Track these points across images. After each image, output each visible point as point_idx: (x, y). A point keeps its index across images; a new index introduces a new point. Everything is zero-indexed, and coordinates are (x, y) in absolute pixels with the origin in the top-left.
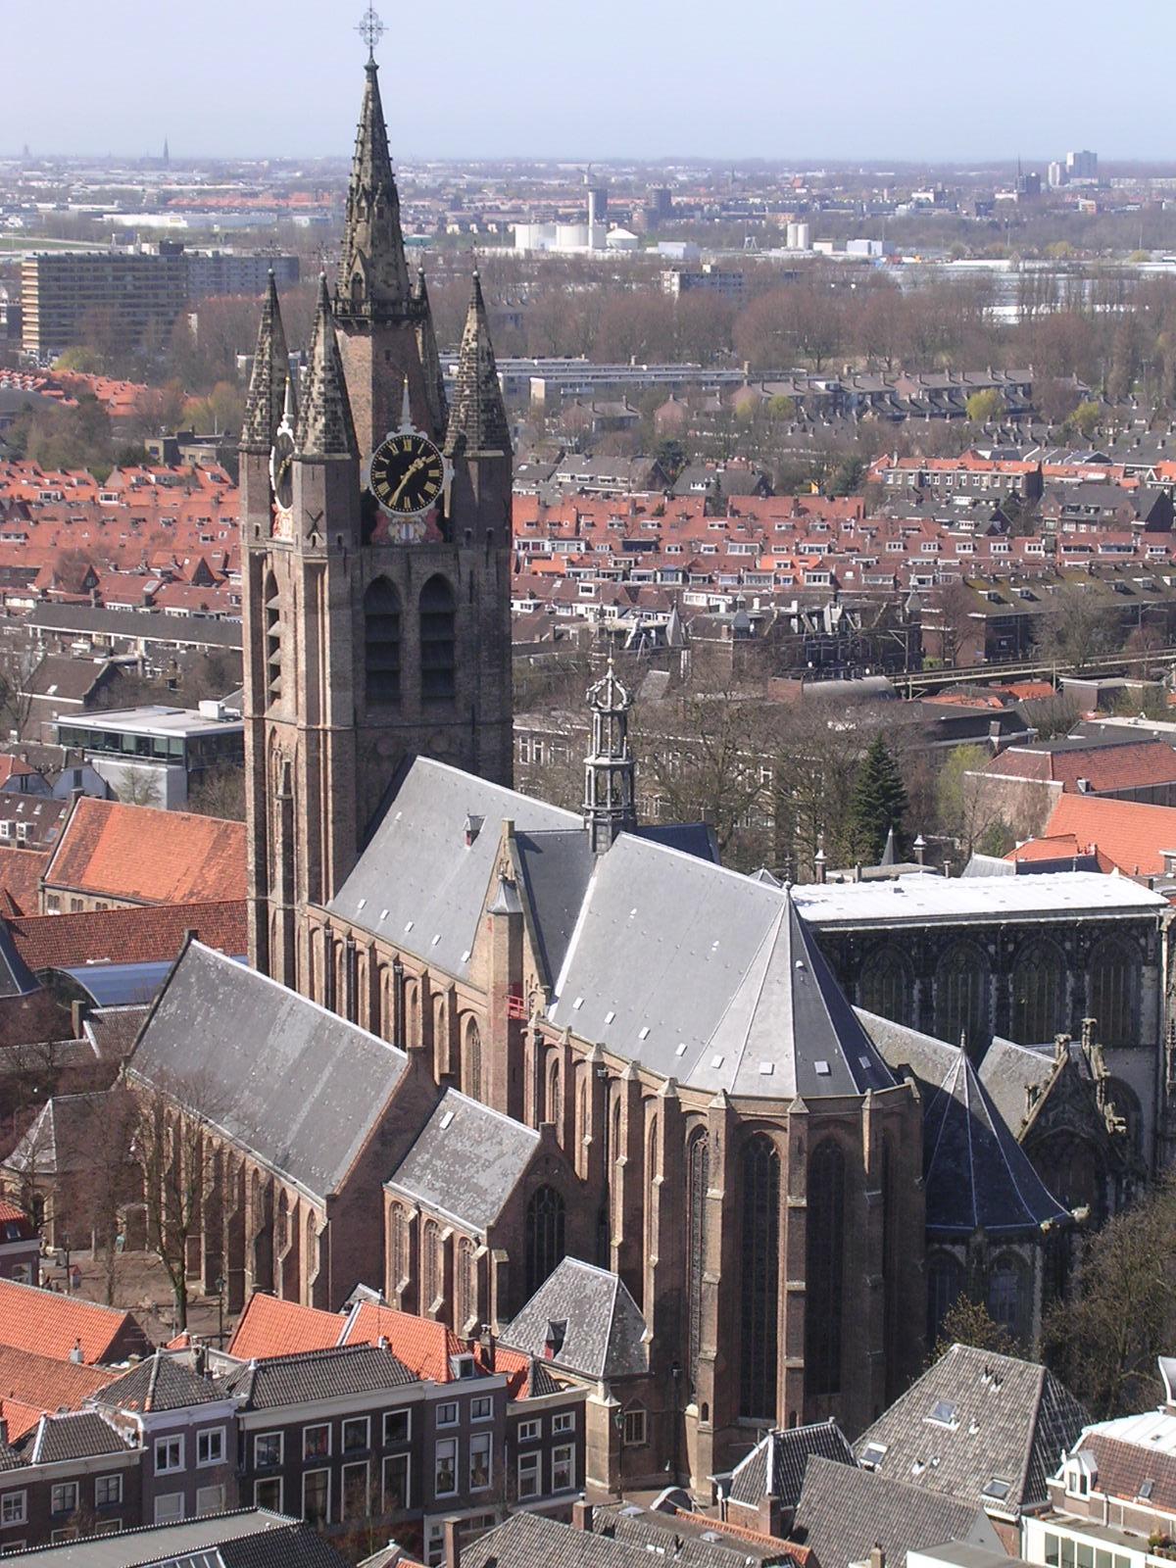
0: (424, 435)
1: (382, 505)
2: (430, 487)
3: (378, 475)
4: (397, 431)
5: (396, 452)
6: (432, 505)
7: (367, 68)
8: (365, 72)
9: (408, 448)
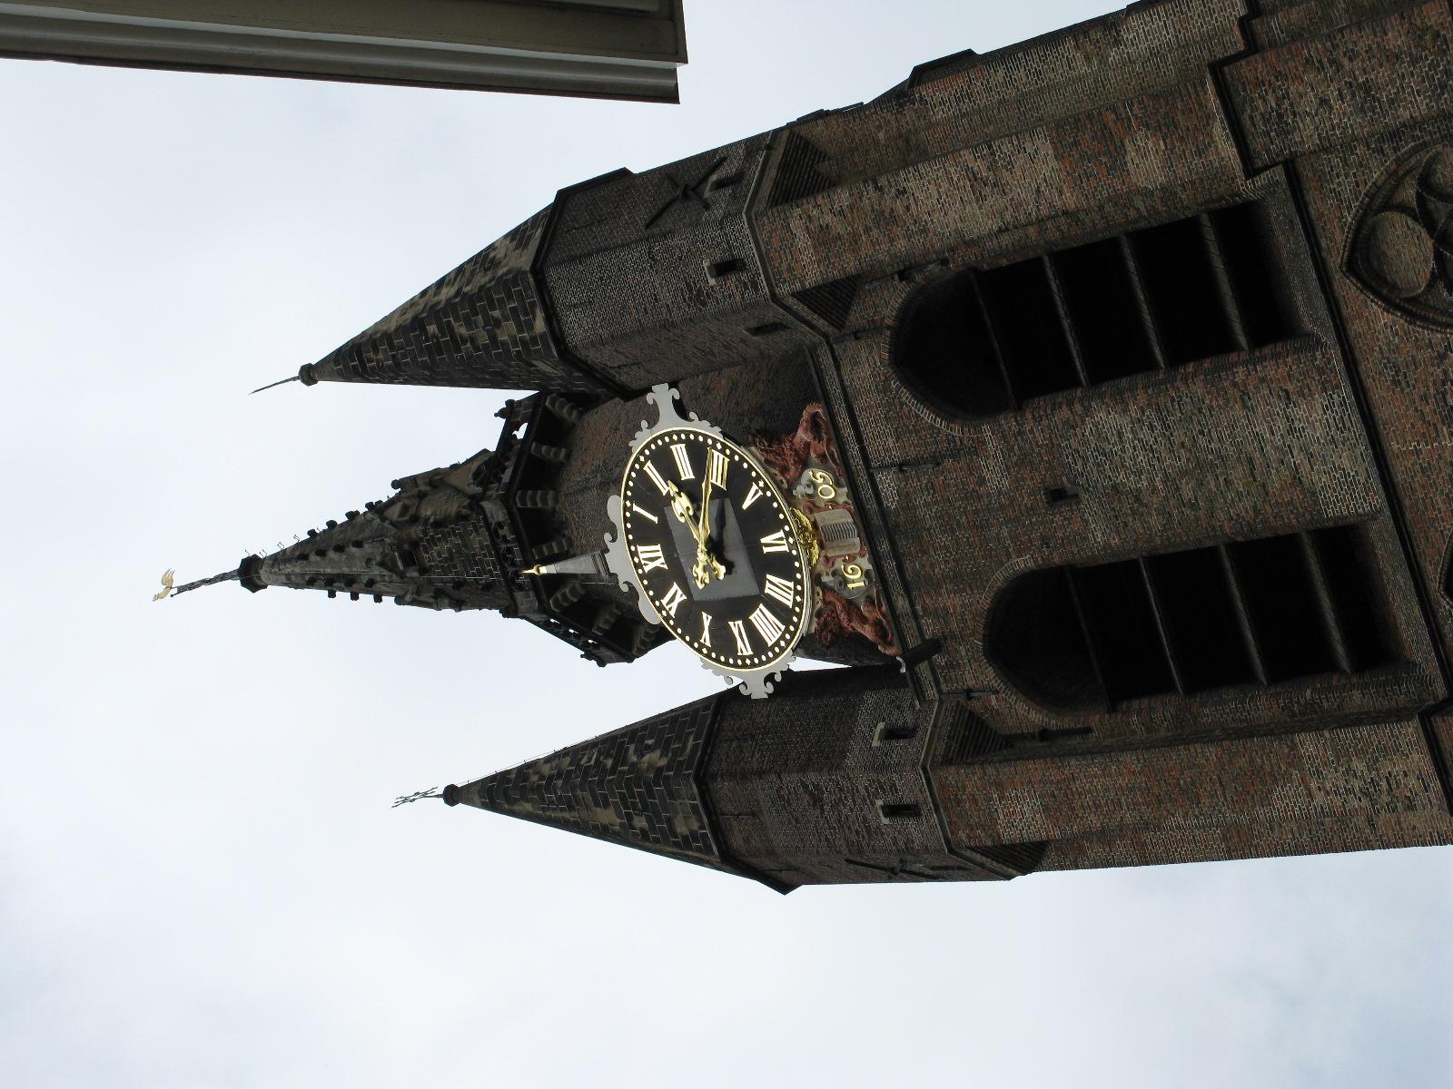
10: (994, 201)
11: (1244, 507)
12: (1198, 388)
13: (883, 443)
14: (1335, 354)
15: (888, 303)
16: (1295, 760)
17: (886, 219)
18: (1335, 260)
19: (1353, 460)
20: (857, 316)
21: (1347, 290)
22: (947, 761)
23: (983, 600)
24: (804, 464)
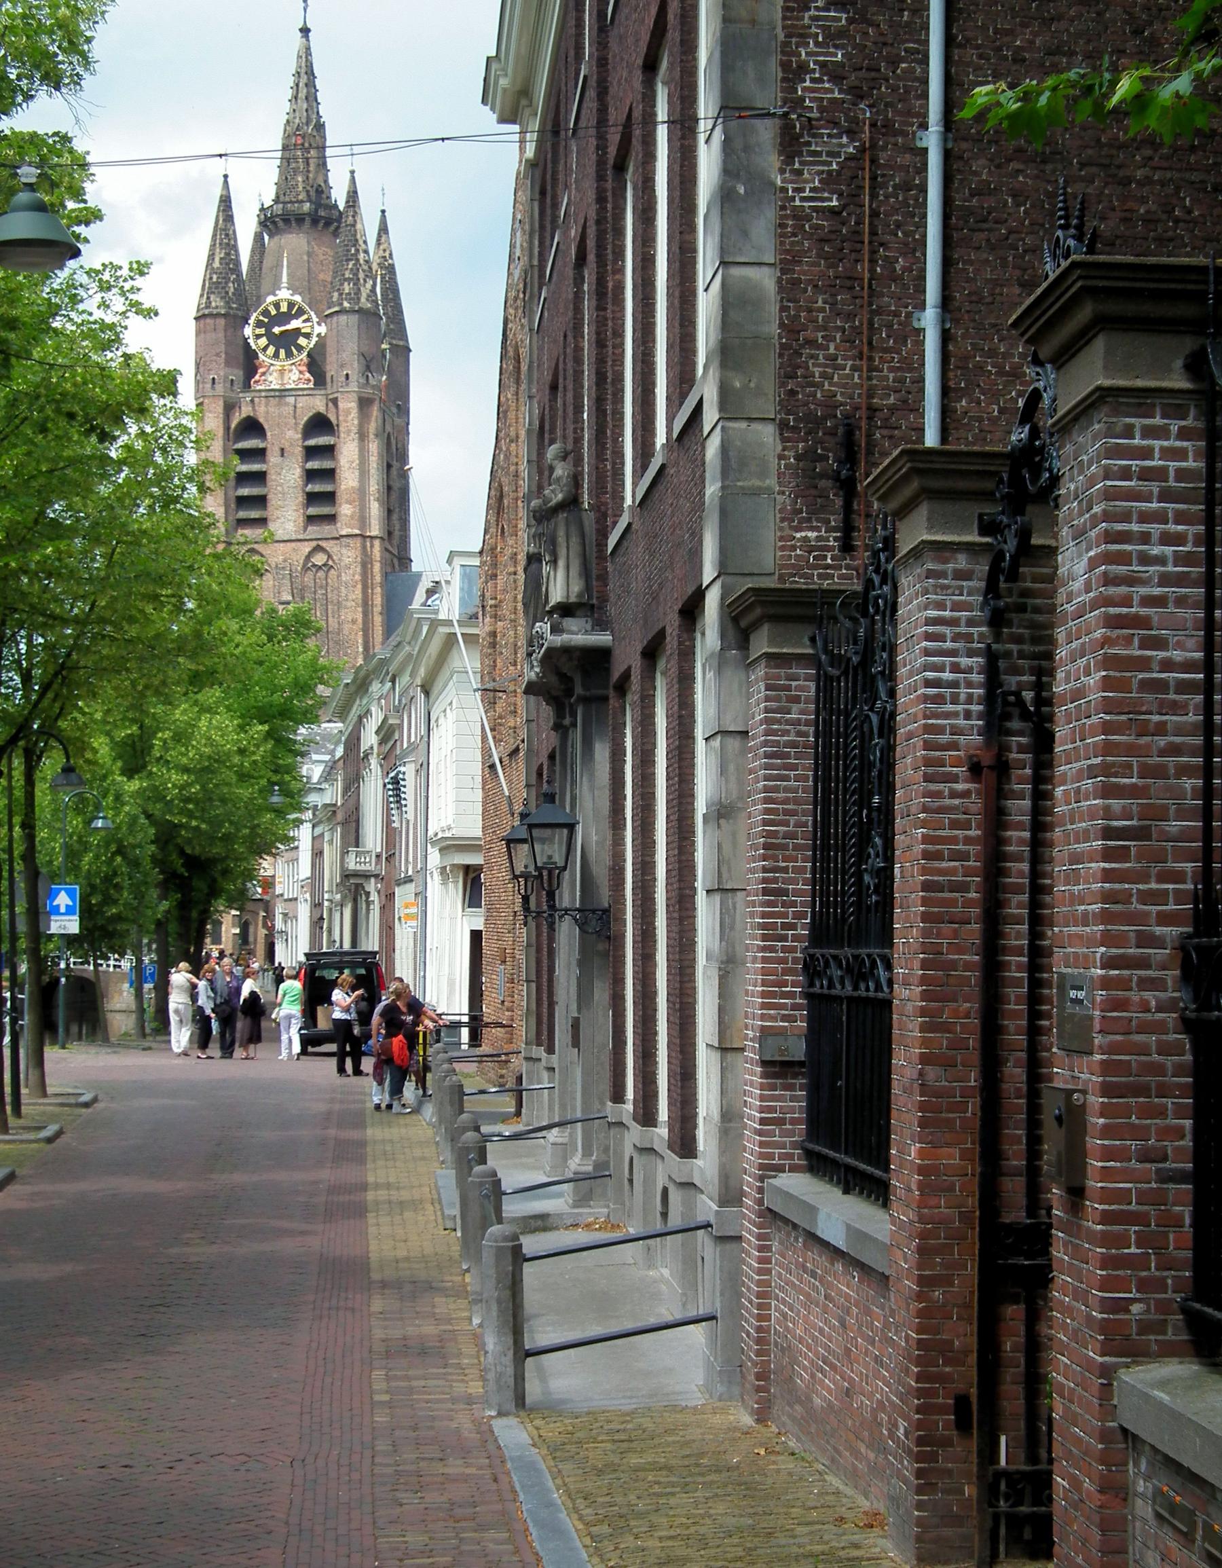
0: (298, 298)
1: (260, 355)
2: (302, 341)
3: (258, 331)
4: (275, 295)
5: (274, 312)
6: (304, 355)
7: (301, 30)
8: (300, 34)
9: (284, 308)
10: (347, 466)
11: (273, 502)
12: (301, 499)
13: (302, 402)
14: (301, 537)
15: (333, 419)
16: (219, 505)
17: (349, 432)
18: (320, 543)
19: (280, 535)
20: (330, 404)
21: (314, 544)
22: (225, 402)
23: (261, 420)
24: (301, 372)
